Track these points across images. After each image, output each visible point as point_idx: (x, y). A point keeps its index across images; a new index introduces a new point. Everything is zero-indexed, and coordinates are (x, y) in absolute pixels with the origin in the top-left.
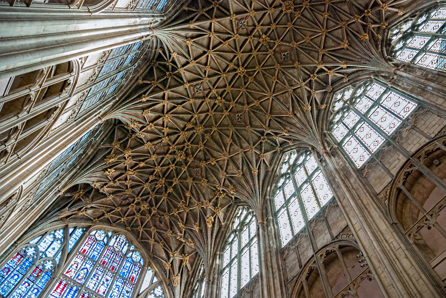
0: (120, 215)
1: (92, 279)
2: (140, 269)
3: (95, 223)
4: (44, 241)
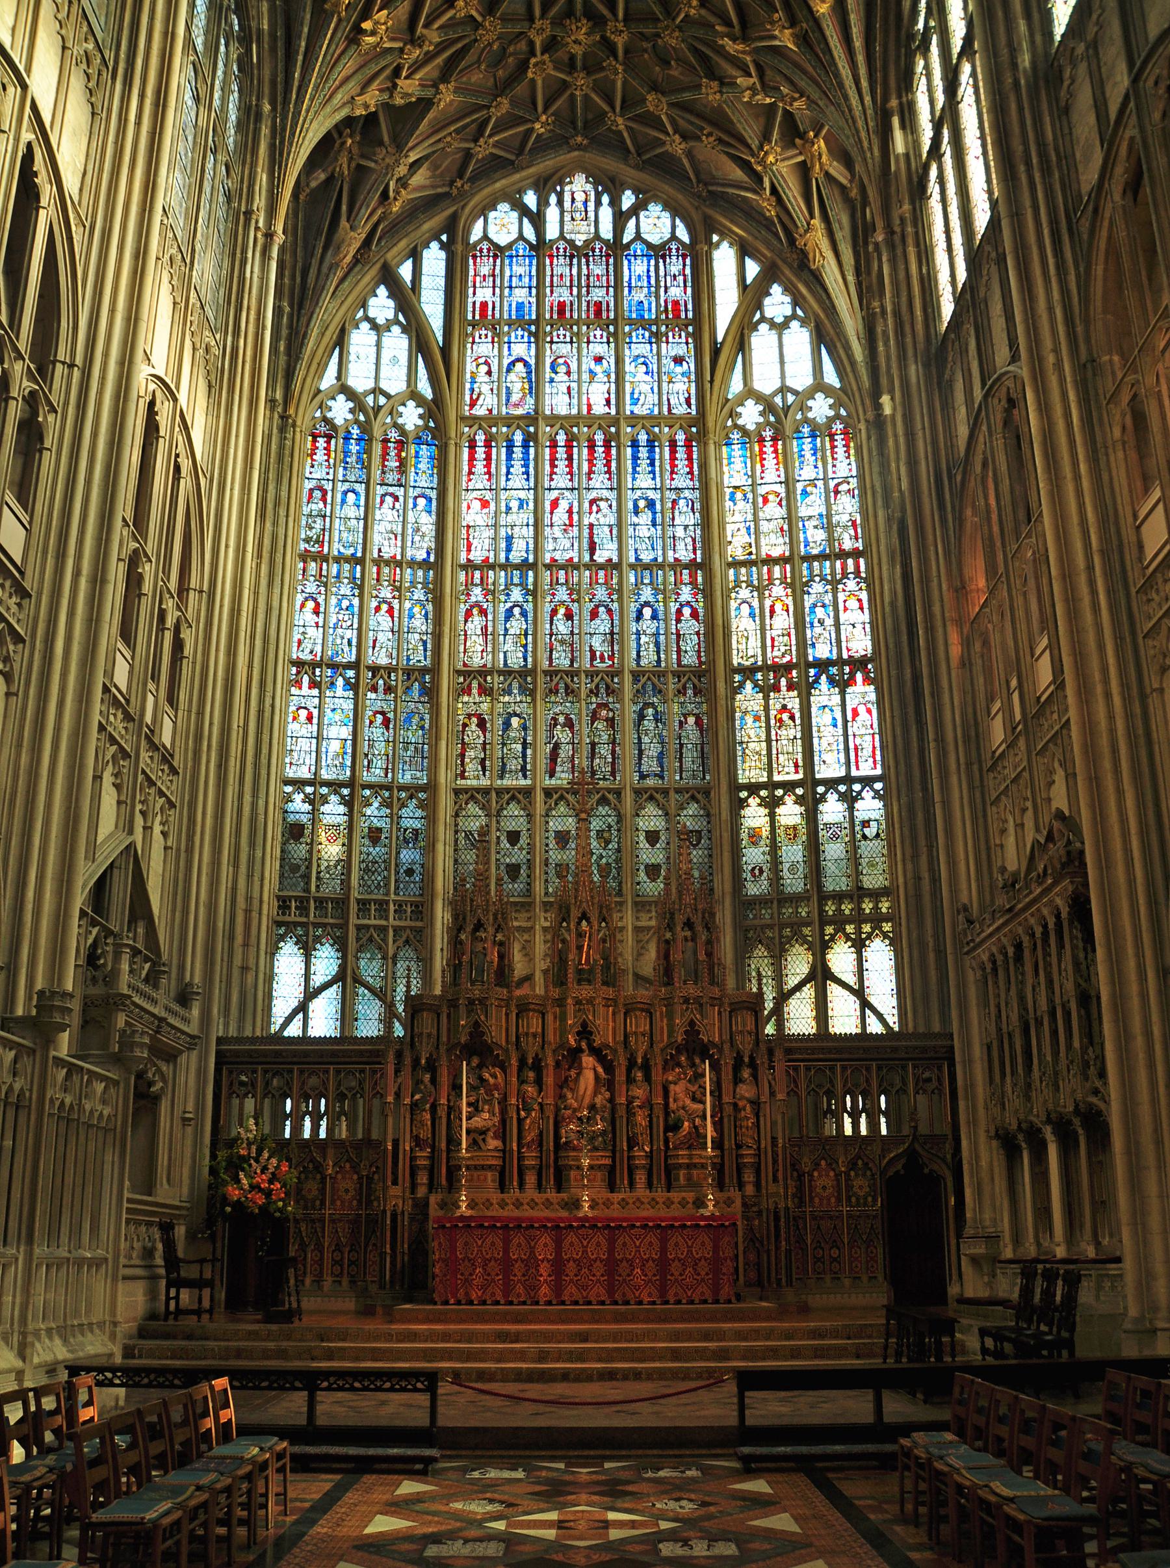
0: (522, 121)
1: (552, 381)
2: (688, 261)
3: (463, 196)
4: (352, 357)
